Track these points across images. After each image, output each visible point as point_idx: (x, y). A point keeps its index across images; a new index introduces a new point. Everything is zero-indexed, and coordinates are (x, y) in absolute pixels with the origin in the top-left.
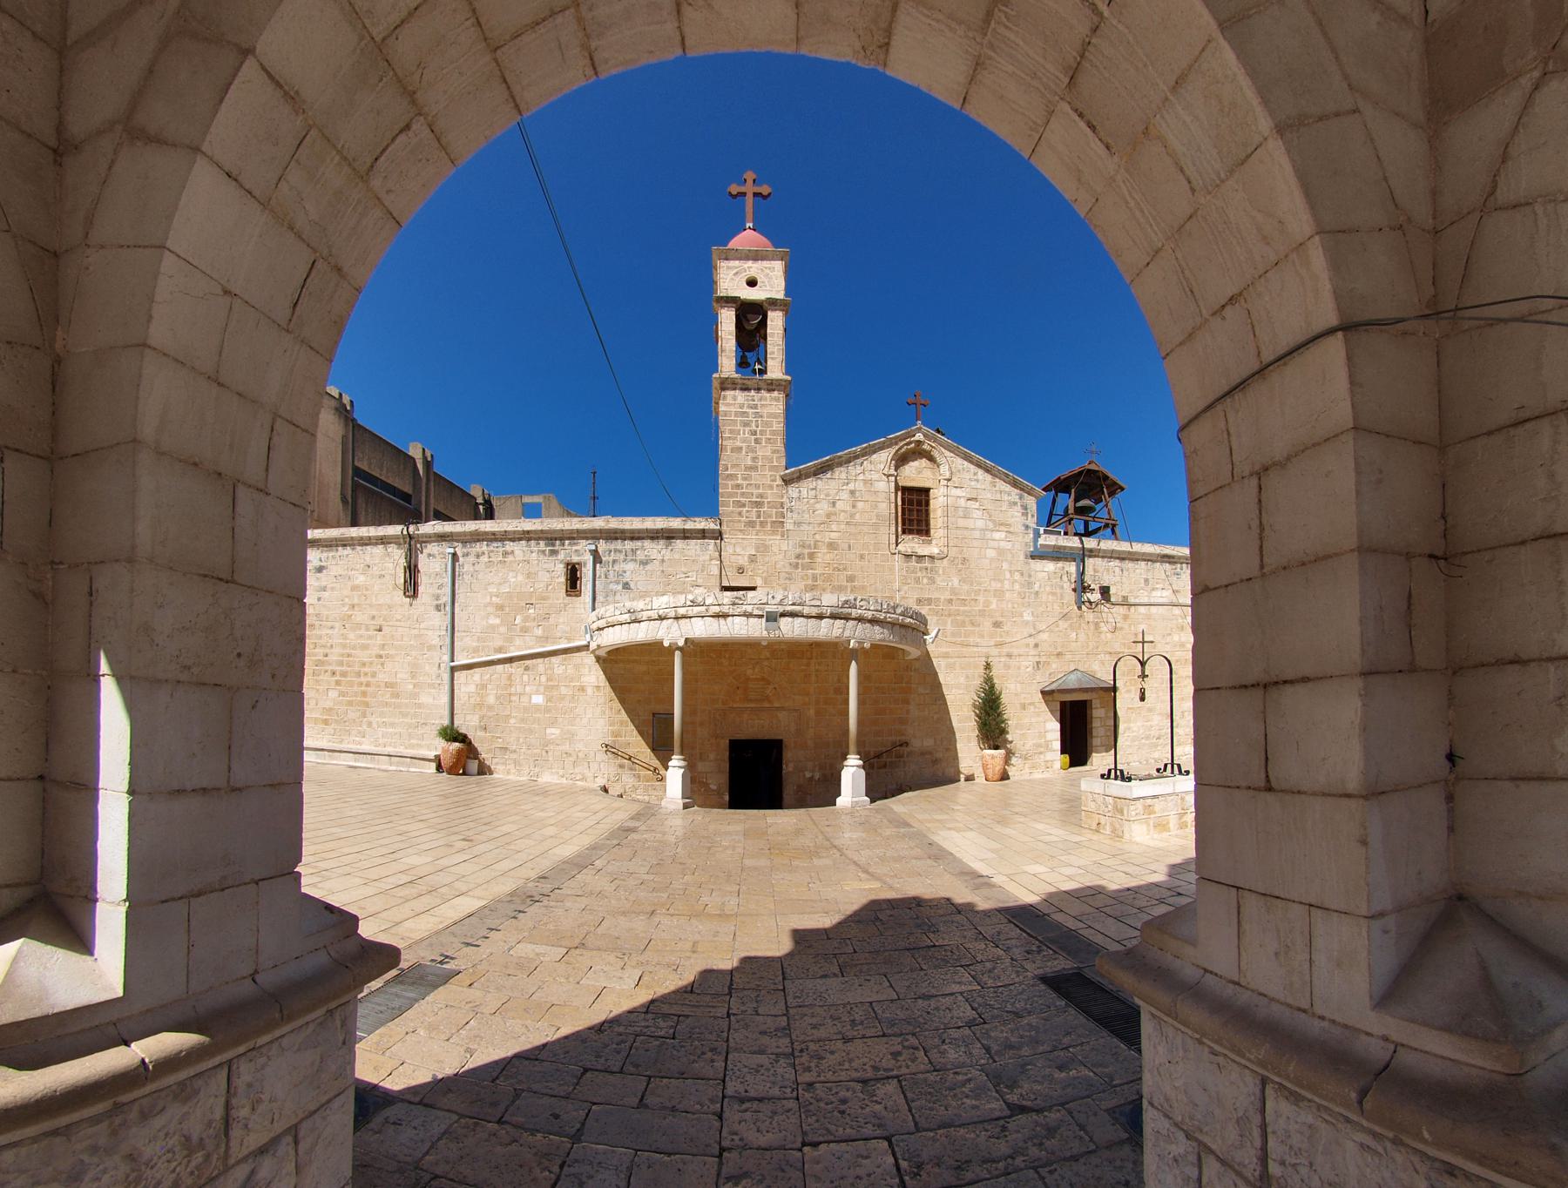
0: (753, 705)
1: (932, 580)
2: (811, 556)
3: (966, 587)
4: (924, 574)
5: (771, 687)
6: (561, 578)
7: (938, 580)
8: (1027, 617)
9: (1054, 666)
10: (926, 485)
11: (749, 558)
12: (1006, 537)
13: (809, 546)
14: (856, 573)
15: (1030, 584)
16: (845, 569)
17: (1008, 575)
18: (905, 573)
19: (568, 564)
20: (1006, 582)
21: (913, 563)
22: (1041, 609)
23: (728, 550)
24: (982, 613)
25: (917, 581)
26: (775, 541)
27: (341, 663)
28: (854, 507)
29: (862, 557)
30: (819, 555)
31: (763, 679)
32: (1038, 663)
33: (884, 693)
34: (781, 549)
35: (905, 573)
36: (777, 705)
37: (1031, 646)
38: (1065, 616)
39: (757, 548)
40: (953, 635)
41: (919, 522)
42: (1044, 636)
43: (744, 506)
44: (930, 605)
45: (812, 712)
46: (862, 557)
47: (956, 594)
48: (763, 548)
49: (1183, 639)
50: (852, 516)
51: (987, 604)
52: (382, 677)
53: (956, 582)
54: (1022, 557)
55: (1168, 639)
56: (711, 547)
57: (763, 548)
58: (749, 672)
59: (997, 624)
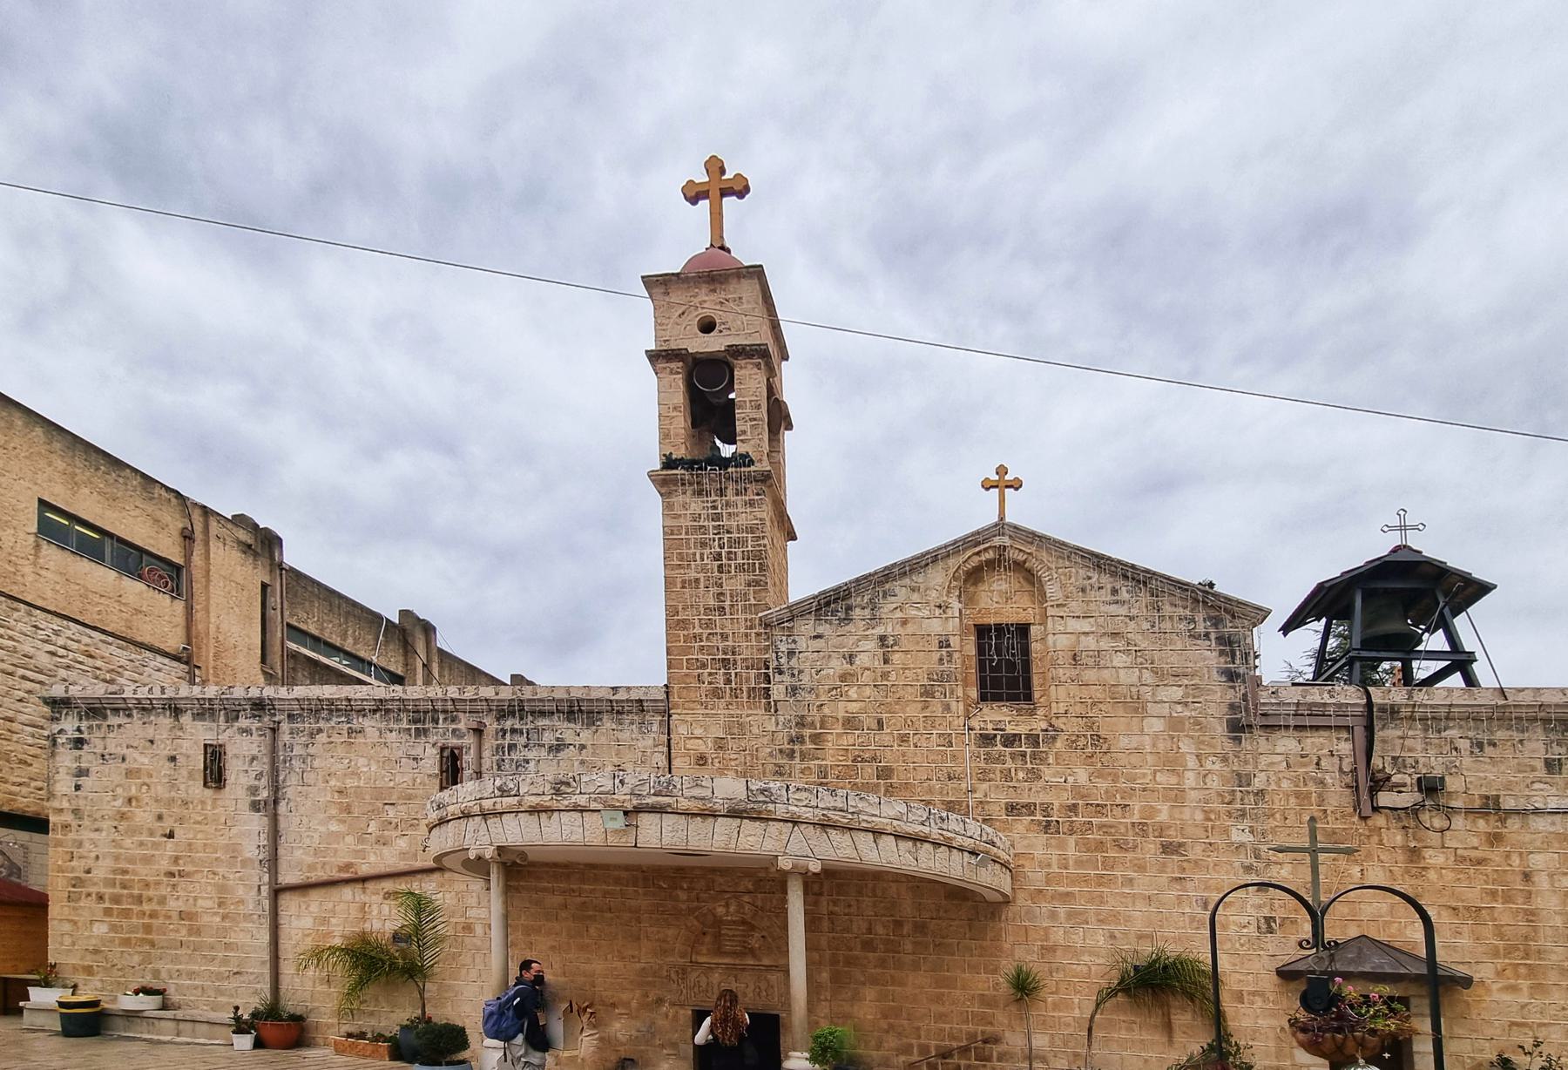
1: (1035, 775)
2: (816, 738)
3: (1103, 785)
4: (1020, 763)
7: (1048, 773)
11: (716, 742)
12: (1186, 695)
13: (812, 725)
14: (895, 765)
15: (1243, 779)
16: (874, 759)
17: (1192, 762)
18: (982, 765)
20: (1189, 774)
23: (681, 730)
24: (1141, 828)
25: (1007, 776)
26: (757, 719)
28: (886, 661)
29: (904, 739)
30: (830, 738)
35: (982, 765)
39: (728, 728)
40: (1079, 863)
41: (1013, 683)
44: (1032, 814)
46: (904, 739)
47: (1083, 797)
48: (738, 728)
50: (885, 675)
51: (1151, 812)
53: (1082, 776)
54: (1220, 729)
56: (655, 728)
57: (738, 728)
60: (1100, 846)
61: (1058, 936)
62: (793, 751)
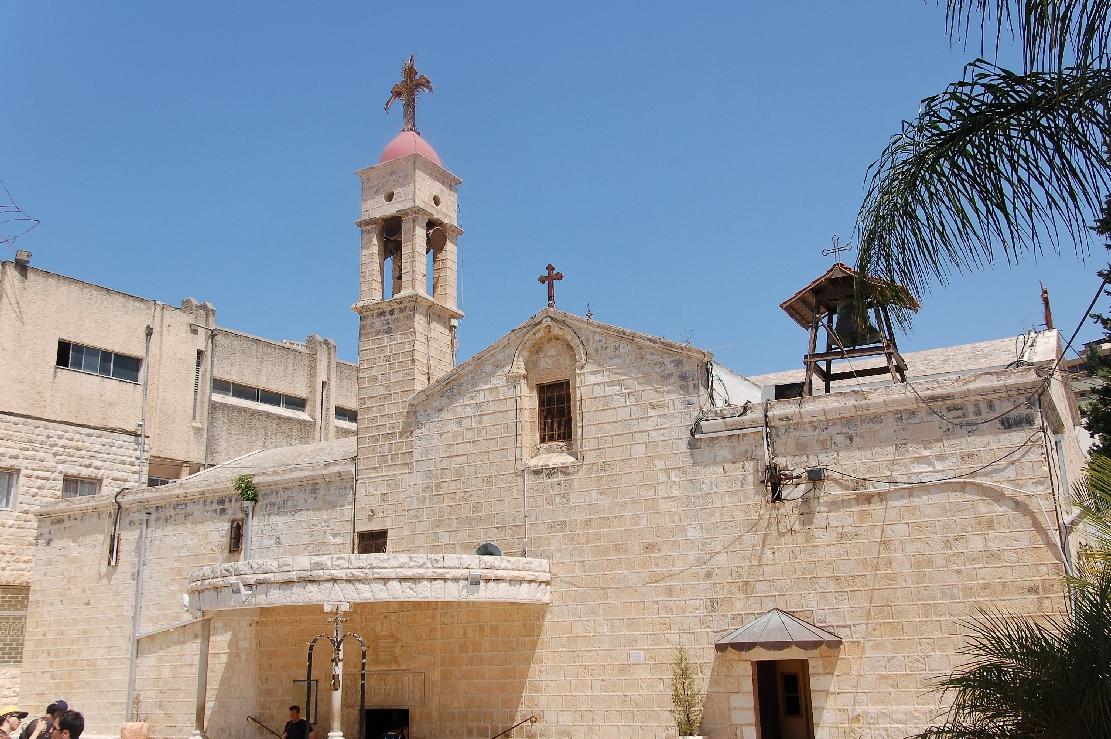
0: (381, 668)
3: (606, 502)
5: (399, 645)
6: (226, 540)
7: (573, 498)
8: (692, 533)
9: (739, 605)
10: (560, 377)
17: (662, 478)
19: (233, 522)
21: (543, 479)
22: (717, 518)
27: (55, 644)
31: (392, 636)
32: (713, 601)
33: (513, 650)
34: (412, 481)
36: (403, 667)
37: (702, 575)
38: (753, 526)
42: (722, 559)
43: (377, 440)
45: (436, 675)
48: (394, 484)
49: (994, 547)
52: (86, 655)
53: (594, 493)
55: (959, 548)
58: (378, 629)
59: (649, 548)
60: (605, 551)
61: (579, 630)
62: (425, 498)
